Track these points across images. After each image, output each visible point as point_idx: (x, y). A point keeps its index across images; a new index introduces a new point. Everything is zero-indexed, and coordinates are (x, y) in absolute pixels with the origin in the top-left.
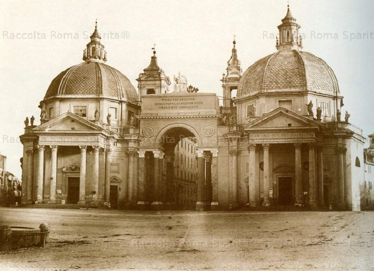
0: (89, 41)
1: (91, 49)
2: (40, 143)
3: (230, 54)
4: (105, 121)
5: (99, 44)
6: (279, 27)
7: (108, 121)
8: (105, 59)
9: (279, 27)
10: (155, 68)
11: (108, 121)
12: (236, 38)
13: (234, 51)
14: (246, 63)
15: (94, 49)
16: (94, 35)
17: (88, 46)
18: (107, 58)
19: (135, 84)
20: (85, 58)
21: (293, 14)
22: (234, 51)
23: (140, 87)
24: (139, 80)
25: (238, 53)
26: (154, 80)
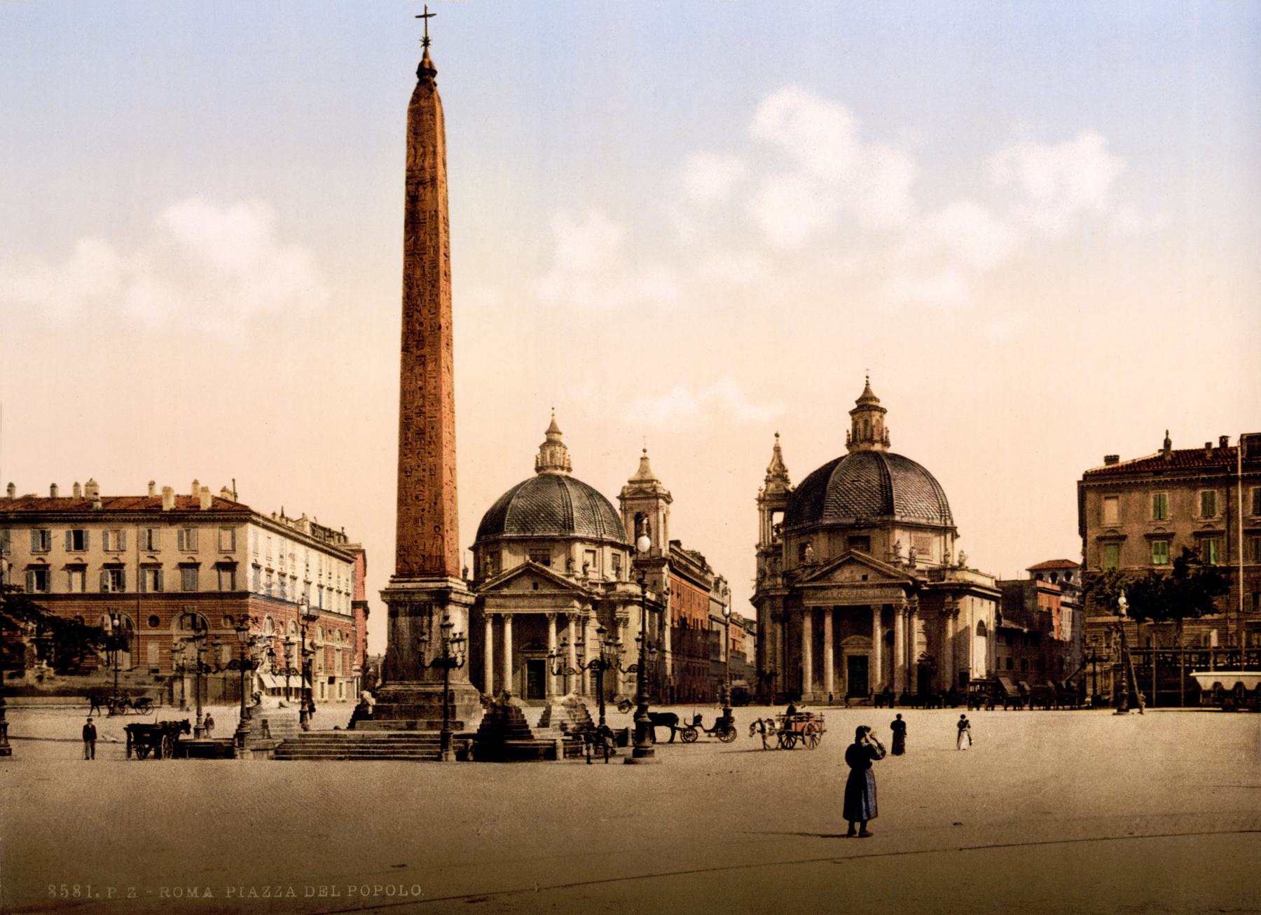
0: (544, 439)
1: (548, 452)
2: (488, 611)
3: (771, 453)
4: (580, 575)
5: (560, 444)
6: (852, 413)
7: (585, 573)
8: (569, 470)
9: (852, 413)
10: (647, 477)
11: (585, 573)
12: (780, 439)
13: (777, 450)
14: (796, 479)
15: (552, 455)
16: (552, 430)
17: (543, 447)
18: (573, 466)
19: (617, 504)
20: (538, 469)
21: (875, 391)
22: (777, 450)
23: (624, 511)
24: (622, 498)
25: (784, 453)
26: (648, 498)
